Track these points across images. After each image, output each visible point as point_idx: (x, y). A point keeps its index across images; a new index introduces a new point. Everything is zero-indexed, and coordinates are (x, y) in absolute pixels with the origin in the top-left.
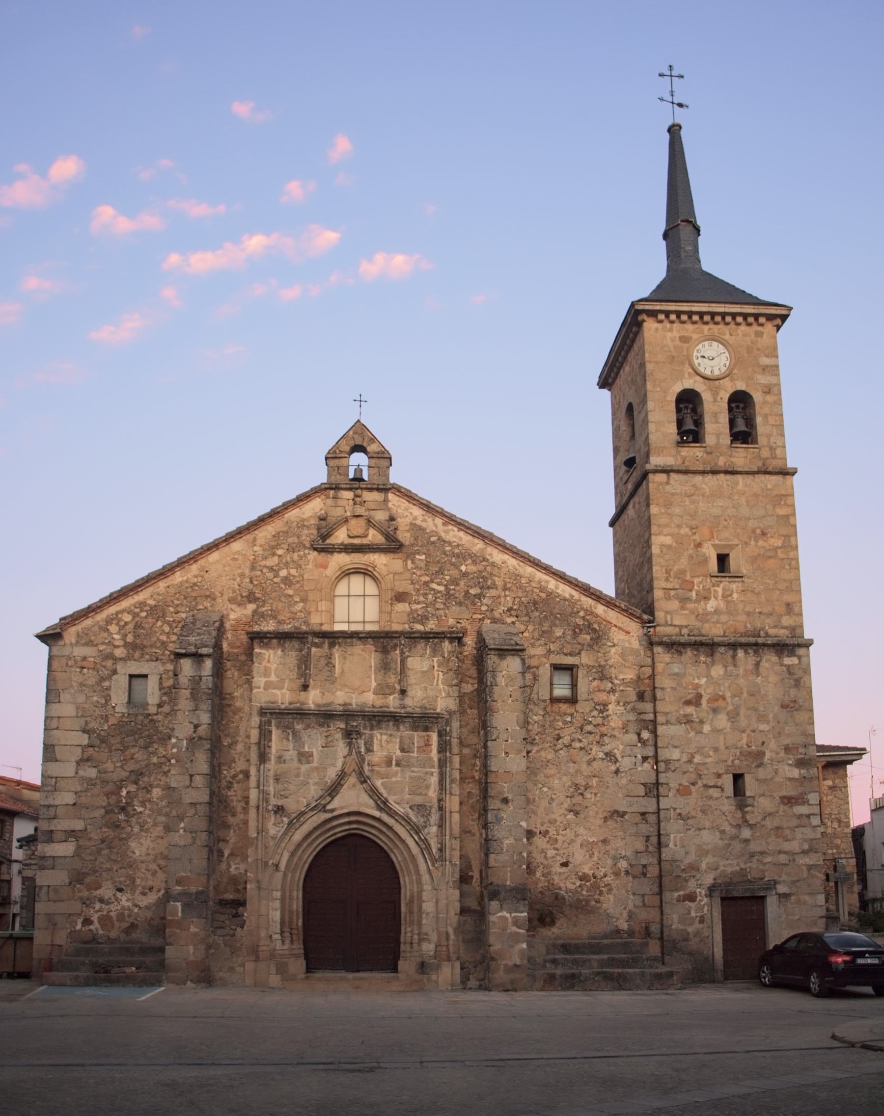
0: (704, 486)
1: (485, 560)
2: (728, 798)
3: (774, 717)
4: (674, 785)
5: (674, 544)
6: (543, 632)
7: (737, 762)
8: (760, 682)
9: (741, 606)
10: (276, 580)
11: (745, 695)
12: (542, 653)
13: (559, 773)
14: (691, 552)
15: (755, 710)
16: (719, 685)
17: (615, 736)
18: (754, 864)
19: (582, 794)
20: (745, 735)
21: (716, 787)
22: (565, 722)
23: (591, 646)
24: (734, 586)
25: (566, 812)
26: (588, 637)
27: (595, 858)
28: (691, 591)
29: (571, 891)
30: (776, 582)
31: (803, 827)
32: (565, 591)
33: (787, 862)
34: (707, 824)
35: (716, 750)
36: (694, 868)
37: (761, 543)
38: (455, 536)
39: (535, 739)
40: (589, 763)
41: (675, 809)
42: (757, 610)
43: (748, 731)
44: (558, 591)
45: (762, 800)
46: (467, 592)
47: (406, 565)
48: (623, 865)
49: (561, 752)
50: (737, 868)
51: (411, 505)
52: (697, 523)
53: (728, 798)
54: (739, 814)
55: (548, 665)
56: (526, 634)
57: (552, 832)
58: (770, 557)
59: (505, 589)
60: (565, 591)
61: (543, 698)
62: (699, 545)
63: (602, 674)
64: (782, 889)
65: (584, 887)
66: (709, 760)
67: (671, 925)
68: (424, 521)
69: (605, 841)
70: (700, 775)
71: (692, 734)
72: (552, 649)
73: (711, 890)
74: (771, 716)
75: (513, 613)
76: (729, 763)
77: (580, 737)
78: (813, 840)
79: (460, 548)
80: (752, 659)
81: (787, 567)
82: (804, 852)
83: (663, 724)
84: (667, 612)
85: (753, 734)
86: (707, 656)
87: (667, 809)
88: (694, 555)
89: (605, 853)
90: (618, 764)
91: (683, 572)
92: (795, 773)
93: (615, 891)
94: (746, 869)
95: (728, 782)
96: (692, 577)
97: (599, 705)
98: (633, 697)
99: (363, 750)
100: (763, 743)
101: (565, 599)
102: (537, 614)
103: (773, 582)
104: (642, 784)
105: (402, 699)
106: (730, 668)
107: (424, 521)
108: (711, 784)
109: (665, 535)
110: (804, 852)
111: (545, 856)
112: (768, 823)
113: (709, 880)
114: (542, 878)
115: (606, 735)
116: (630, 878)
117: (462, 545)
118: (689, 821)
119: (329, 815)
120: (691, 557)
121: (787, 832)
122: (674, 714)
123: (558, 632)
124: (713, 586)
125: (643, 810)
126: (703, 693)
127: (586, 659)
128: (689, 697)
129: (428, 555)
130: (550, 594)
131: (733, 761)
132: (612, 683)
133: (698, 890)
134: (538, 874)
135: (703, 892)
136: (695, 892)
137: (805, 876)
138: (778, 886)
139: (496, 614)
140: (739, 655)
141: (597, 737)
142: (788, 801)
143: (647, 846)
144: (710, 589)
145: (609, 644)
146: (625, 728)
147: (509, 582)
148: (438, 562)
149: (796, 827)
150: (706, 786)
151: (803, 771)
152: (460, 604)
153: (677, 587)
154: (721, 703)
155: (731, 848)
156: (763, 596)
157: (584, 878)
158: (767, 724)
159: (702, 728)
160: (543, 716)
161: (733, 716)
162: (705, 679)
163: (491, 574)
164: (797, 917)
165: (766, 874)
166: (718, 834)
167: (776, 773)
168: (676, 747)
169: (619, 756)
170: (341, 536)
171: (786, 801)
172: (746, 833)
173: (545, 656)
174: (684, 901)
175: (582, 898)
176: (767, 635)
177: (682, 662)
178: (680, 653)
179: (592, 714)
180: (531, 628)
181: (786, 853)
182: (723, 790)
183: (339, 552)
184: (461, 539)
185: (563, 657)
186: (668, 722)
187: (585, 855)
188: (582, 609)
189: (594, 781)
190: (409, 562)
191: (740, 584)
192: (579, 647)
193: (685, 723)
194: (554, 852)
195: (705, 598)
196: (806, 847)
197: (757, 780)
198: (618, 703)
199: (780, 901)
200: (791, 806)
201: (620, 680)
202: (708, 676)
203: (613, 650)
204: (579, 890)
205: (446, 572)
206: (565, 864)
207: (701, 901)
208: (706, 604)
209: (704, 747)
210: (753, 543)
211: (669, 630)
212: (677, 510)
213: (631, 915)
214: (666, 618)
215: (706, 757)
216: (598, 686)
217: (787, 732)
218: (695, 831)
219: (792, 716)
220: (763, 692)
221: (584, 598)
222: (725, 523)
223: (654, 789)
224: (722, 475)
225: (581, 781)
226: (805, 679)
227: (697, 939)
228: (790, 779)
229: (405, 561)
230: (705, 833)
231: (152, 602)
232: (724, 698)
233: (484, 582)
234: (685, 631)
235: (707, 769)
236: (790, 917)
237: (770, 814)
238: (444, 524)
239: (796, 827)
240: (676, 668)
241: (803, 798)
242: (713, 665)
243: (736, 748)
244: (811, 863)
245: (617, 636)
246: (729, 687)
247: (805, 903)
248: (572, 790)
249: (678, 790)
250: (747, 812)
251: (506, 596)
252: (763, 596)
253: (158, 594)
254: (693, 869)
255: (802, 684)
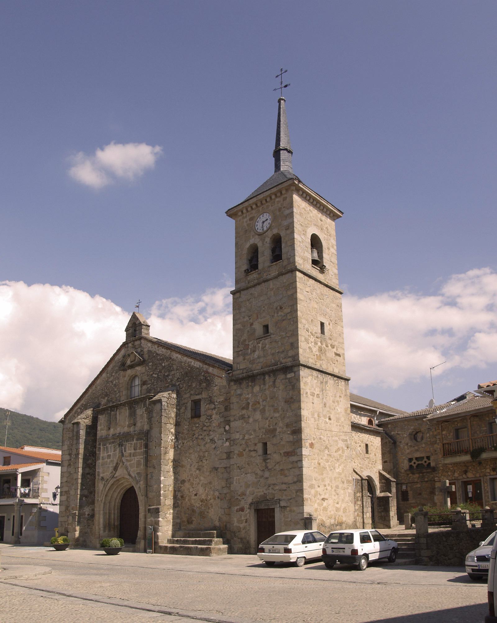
0: (255, 292)
1: (171, 358)
2: (259, 456)
3: (281, 409)
4: (236, 452)
5: (242, 328)
6: (189, 386)
7: (264, 436)
8: (275, 391)
9: (270, 351)
10: (112, 386)
11: (268, 399)
12: (189, 396)
13: (194, 451)
14: (249, 329)
15: (273, 406)
16: (257, 396)
17: (215, 430)
18: (271, 491)
19: (202, 461)
20: (267, 421)
21: (254, 450)
22: (196, 427)
23: (206, 388)
24: (267, 341)
25: (196, 470)
26: (205, 384)
27: (206, 492)
28: (248, 349)
29: (198, 507)
30: (286, 333)
31: (294, 468)
32: (197, 364)
33: (286, 488)
34: (250, 471)
35: (255, 431)
36: (243, 494)
37: (280, 313)
38: (161, 351)
39: (185, 437)
40: (204, 445)
41: (236, 464)
42: (277, 351)
43: (269, 419)
44: (195, 365)
45: (275, 455)
46: (164, 375)
47: (146, 369)
48: (217, 494)
49: (195, 441)
50: (263, 493)
51: (148, 342)
52: (251, 313)
53: (259, 456)
54: (264, 464)
55: (190, 401)
56: (183, 389)
57: (191, 480)
58: (284, 320)
59: (177, 370)
60: (197, 364)
61: (188, 417)
62: (252, 324)
63: (211, 402)
64: (283, 504)
65: (203, 505)
66: (252, 437)
67: (234, 524)
68: (152, 347)
69: (210, 483)
70: (248, 445)
71: (245, 424)
72: (192, 393)
73: (251, 504)
74: (280, 408)
75: (179, 380)
76: (260, 437)
77: (202, 433)
78: (299, 475)
79: (163, 356)
80: (272, 379)
81: (292, 323)
82: (295, 483)
83: (232, 421)
84: (238, 363)
85: (271, 420)
86: (252, 382)
87: (233, 465)
88: (250, 331)
89: (210, 489)
90: (216, 444)
91: (245, 340)
92: (291, 438)
93: (214, 507)
94: (266, 494)
95: (260, 447)
96: (248, 342)
97: (208, 416)
98: (223, 410)
99: (123, 451)
100: (276, 424)
101: (197, 368)
102: (187, 378)
103: (285, 333)
104: (226, 453)
105: (134, 428)
106: (262, 386)
107: (152, 347)
108: (252, 449)
109: (238, 324)
110: (295, 483)
111: (189, 491)
112: (278, 468)
113: (250, 500)
114: (188, 502)
115: (211, 431)
116: (219, 500)
117: (163, 355)
118: (242, 470)
119: (115, 480)
120: (248, 332)
121: (286, 472)
122: (237, 415)
123: (194, 385)
124: (257, 344)
125: (225, 466)
126: (250, 402)
127: (204, 395)
128: (244, 405)
129: (153, 362)
130: (192, 368)
131: (262, 436)
132: (214, 404)
133: (245, 506)
134: (187, 500)
135: (248, 506)
136: (244, 507)
137: (294, 496)
138: (281, 502)
139: (173, 382)
140: (266, 378)
141: (208, 433)
142: (287, 454)
143: (227, 484)
144: (256, 346)
145: (215, 385)
146: (219, 426)
147: (179, 366)
148: (156, 364)
149: (291, 469)
150: (250, 451)
151: (295, 437)
152: (161, 381)
153: (242, 349)
154: (258, 406)
155: (260, 483)
156: (280, 343)
157: (202, 501)
158: (278, 412)
159: (249, 420)
160: (188, 425)
161: (263, 411)
162: (251, 394)
163: (172, 364)
164: (289, 520)
165: (276, 495)
166: (254, 475)
167: (282, 440)
168: (238, 432)
169: (216, 440)
170: (129, 362)
171: (286, 455)
172: (267, 474)
173: (190, 397)
174: (239, 511)
175: (202, 510)
176: (281, 363)
177: (241, 388)
178: (240, 384)
179: (206, 422)
180: (184, 385)
181: (285, 483)
182: (257, 452)
183: (128, 369)
184: (163, 352)
185: (196, 396)
186: (235, 420)
187: (203, 490)
188: (203, 371)
189: (207, 452)
190: (147, 367)
191: (269, 339)
192: (201, 390)
193: (242, 419)
194: (192, 489)
195: (254, 351)
196: (295, 480)
197: (273, 444)
198: (217, 414)
199: (281, 511)
200: (288, 457)
201: (218, 402)
202: (252, 393)
203: (216, 388)
204: (201, 507)
205: (158, 368)
206: (196, 495)
207: (246, 511)
208: (254, 355)
209: (250, 430)
210: (276, 315)
211: (238, 372)
212: (243, 309)
213: (220, 519)
214: (237, 366)
215: (250, 435)
216: (208, 407)
217: (287, 416)
218: (244, 475)
219: (290, 407)
220: (276, 396)
221: (205, 366)
222: (264, 309)
223: (229, 455)
224: (263, 284)
225: (201, 454)
226: (297, 384)
227: (244, 531)
228: (288, 442)
229: (146, 367)
230: (248, 475)
231: (84, 403)
232: (259, 403)
233: (169, 369)
234: (245, 371)
235: (251, 442)
236: (286, 520)
237: (278, 463)
238: (158, 347)
239: (291, 469)
240: (239, 392)
241: (294, 452)
242: (255, 386)
243: (263, 429)
244: (298, 489)
245: (217, 381)
246: (261, 396)
247: (294, 511)
248: (198, 459)
249: (238, 454)
250: (267, 463)
251: (177, 373)
252: (280, 343)
253: (86, 400)
254: (243, 495)
255: (296, 387)
